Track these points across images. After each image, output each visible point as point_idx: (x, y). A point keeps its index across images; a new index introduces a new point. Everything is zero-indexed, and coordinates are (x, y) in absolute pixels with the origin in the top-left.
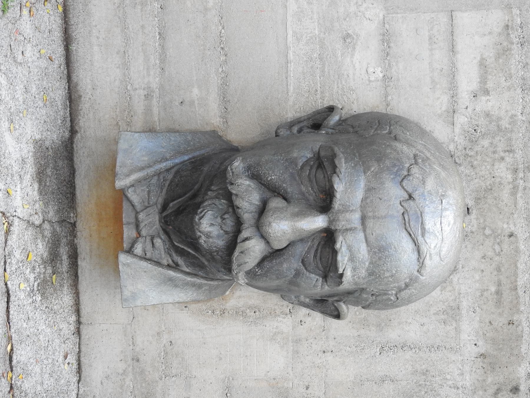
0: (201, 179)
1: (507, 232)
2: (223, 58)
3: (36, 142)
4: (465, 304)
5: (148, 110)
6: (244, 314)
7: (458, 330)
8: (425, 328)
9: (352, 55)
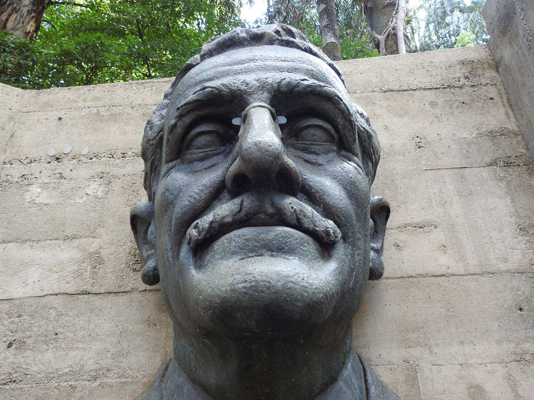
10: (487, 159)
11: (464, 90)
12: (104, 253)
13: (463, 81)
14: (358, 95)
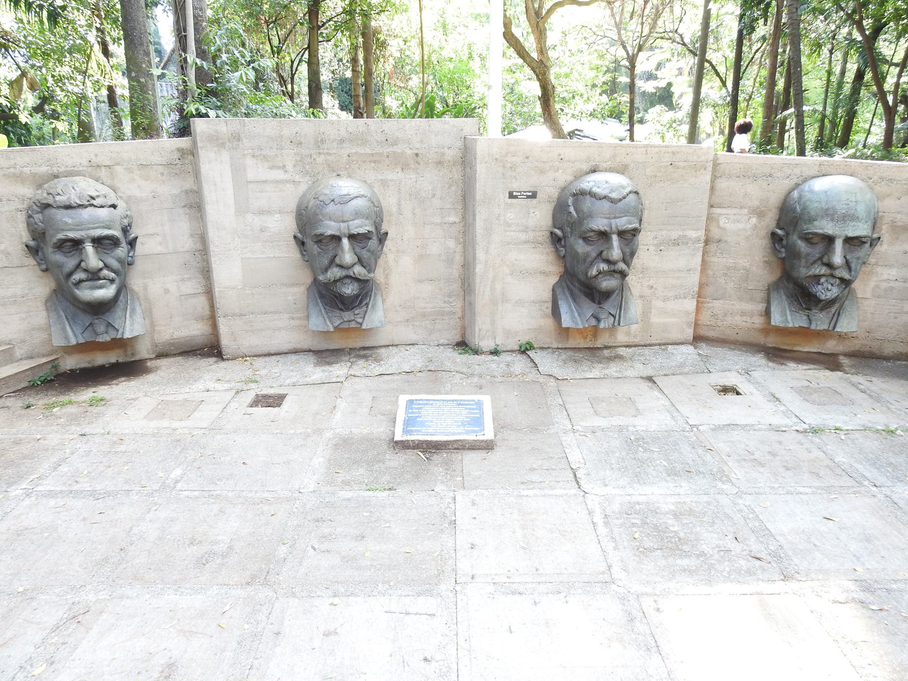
0: (328, 294)
1: (347, 158)
2: (274, 286)
3: (315, 366)
4: (380, 177)
5: (299, 318)
6: (387, 275)
7: (392, 181)
8: (391, 195)
9: (270, 228)
10: (183, 205)
11: (177, 167)
12: (9, 250)
13: (178, 161)
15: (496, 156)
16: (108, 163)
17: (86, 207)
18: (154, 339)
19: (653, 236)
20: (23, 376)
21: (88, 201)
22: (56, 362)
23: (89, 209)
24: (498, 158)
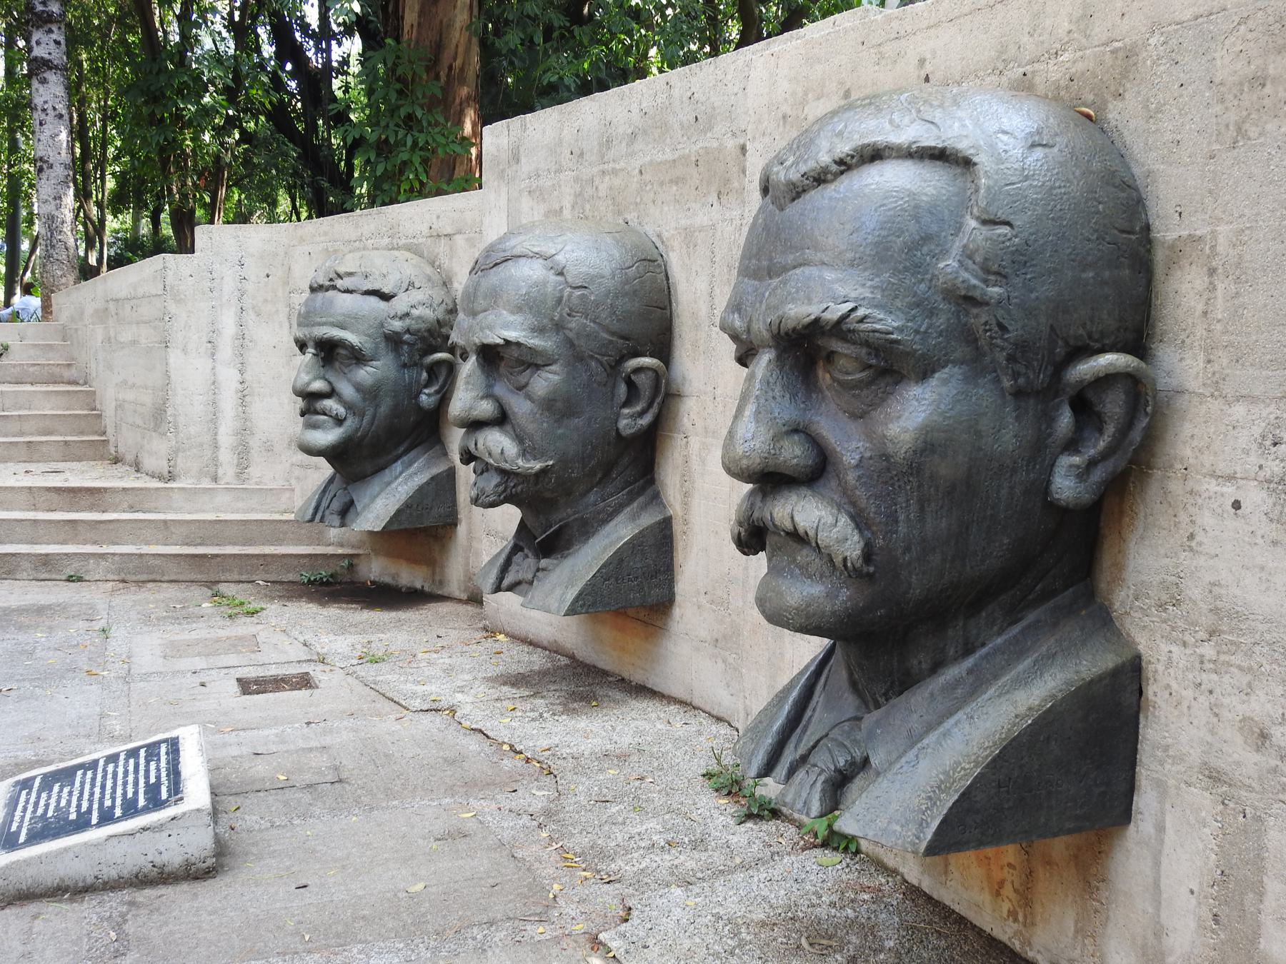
1: (639, 177)
4: (683, 222)
7: (701, 229)
14: (466, 236)
15: (785, 108)
16: (449, 230)
17: (327, 290)
18: (467, 564)
19: (1257, 431)
20: (296, 563)
21: (331, 280)
22: (355, 561)
23: (331, 293)
24: (789, 113)
